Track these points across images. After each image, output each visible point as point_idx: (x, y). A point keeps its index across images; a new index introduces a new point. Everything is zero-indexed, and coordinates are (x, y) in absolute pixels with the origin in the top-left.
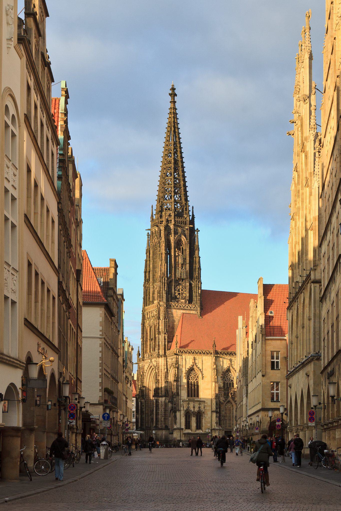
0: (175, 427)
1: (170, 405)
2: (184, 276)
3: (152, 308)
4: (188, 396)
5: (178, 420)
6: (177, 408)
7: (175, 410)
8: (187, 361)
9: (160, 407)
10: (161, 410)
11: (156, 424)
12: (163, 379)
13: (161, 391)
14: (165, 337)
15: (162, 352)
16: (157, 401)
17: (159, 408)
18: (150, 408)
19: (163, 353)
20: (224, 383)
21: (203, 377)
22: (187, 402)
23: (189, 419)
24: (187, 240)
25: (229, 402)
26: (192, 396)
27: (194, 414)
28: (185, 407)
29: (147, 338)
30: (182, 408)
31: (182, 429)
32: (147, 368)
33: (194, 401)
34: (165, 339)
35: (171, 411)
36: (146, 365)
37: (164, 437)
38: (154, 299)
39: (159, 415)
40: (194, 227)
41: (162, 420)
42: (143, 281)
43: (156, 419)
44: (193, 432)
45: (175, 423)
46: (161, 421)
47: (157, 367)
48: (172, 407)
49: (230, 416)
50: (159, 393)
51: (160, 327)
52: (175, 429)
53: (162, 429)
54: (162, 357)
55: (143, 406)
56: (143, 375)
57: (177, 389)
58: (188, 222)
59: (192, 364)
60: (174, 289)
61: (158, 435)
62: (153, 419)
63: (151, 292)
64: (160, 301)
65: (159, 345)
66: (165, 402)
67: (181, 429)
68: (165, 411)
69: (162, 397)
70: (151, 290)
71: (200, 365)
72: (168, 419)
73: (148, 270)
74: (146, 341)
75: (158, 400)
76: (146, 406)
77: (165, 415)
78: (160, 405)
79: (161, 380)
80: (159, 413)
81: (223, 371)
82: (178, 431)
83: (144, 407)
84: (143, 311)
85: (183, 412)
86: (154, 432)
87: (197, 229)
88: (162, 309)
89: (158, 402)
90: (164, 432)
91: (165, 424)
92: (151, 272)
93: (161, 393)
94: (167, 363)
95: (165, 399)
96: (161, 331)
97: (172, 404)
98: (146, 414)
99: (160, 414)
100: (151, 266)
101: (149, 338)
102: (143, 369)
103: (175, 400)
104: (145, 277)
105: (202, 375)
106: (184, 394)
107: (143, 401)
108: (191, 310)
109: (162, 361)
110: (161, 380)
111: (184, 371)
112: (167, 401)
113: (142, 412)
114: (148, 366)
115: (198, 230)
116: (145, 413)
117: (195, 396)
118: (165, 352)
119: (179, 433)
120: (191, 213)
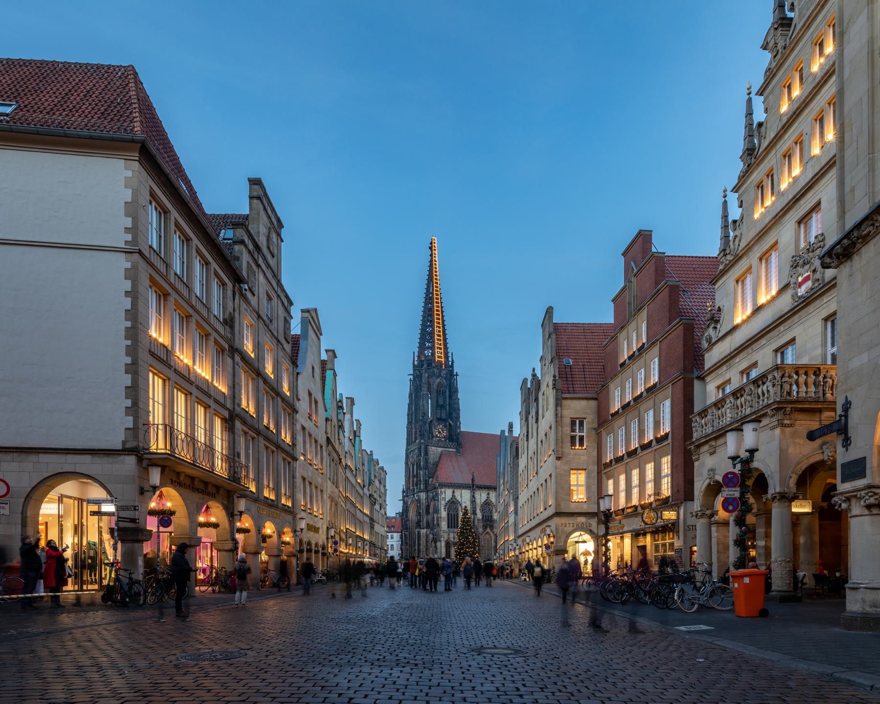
2: (444, 416)
3: (413, 447)
5: (439, 550)
7: (435, 540)
8: (448, 494)
16: (419, 533)
38: (416, 439)
40: (452, 371)
43: (419, 549)
47: (419, 501)
57: (438, 521)
71: (459, 498)
84: (407, 449)
85: (443, 544)
88: (423, 446)
106: (444, 525)
109: (423, 495)
115: (457, 375)
118: (426, 488)
120: (450, 359)
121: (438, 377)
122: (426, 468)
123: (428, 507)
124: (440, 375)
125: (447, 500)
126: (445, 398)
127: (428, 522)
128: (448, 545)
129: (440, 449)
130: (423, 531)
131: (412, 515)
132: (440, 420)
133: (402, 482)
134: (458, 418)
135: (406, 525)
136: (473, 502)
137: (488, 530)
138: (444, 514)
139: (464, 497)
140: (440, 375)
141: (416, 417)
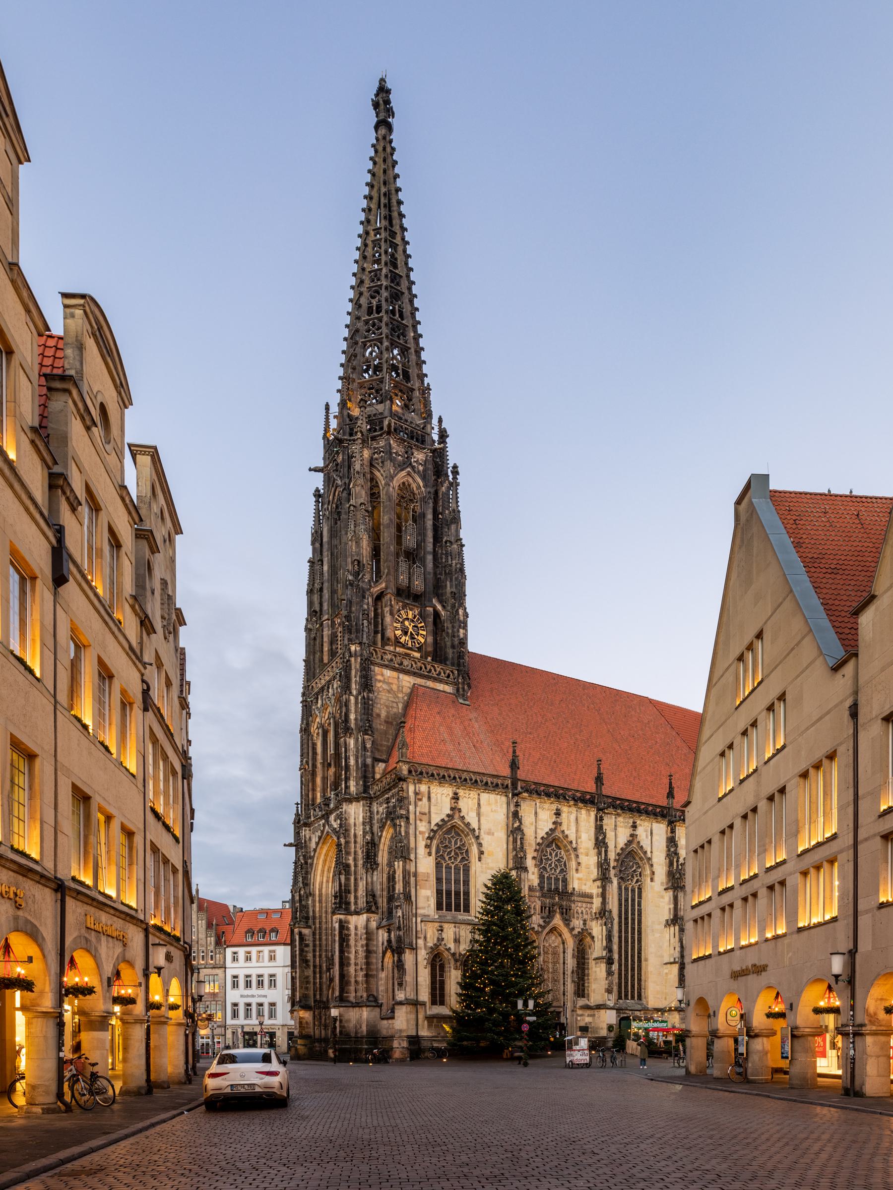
0: (400, 996)
1: (382, 936)
4: (439, 907)
5: (409, 978)
6: (407, 941)
7: (398, 948)
9: (352, 942)
10: (356, 952)
11: (342, 990)
12: (360, 862)
13: (356, 897)
14: (364, 742)
16: (343, 926)
17: (348, 946)
18: (326, 951)
19: (361, 789)
20: (541, 877)
21: (482, 853)
22: (437, 925)
23: (442, 976)
24: (425, 486)
25: (554, 929)
26: (449, 908)
27: (456, 961)
28: (428, 939)
30: (421, 942)
31: (423, 1004)
32: (317, 844)
33: (455, 922)
35: (384, 953)
36: (313, 836)
37: (364, 1028)
39: (349, 964)
41: (360, 979)
42: (305, 615)
43: (342, 976)
46: (356, 982)
47: (344, 829)
48: (389, 941)
49: (555, 971)
50: (348, 904)
51: (352, 716)
52: (401, 1003)
53: (357, 1005)
54: (357, 799)
55: (307, 946)
56: (306, 863)
57: (406, 883)
59: (449, 812)
60: (392, 614)
61: (348, 1021)
62: (331, 980)
63: (326, 639)
64: (350, 640)
65: (347, 767)
66: (367, 927)
67: (415, 1004)
68: (369, 952)
69: (357, 913)
71: (471, 818)
72: (377, 976)
73: (317, 586)
75: (348, 922)
76: (314, 946)
77: (368, 964)
79: (356, 866)
80: (349, 958)
81: (539, 840)
82: (409, 1008)
83: (311, 948)
85: (423, 954)
87: (455, 467)
89: (348, 929)
90: (365, 1014)
91: (367, 989)
92: (326, 585)
93: (356, 903)
94: (371, 818)
95: (368, 920)
96: (353, 726)
97: (389, 932)
98: (315, 966)
99: (352, 961)
102: (306, 846)
103: (400, 913)
104: (310, 604)
105: (480, 845)
106: (426, 898)
107: (306, 931)
109: (355, 812)
110: (356, 866)
112: (373, 925)
113: (304, 961)
114: (320, 838)
116: (311, 964)
117: (458, 909)
118: (366, 788)
119: (413, 1016)
121: (401, 467)
122: (367, 727)
123: (371, 848)
124: (407, 463)
125: (436, 819)
126: (422, 533)
127: (371, 895)
128: (437, 962)
130: (357, 922)
131: (323, 880)
132: (405, 594)
134: (459, 596)
135: (304, 908)
136: (515, 832)
137: (557, 920)
138: (425, 864)
139: (488, 812)
140: (407, 463)
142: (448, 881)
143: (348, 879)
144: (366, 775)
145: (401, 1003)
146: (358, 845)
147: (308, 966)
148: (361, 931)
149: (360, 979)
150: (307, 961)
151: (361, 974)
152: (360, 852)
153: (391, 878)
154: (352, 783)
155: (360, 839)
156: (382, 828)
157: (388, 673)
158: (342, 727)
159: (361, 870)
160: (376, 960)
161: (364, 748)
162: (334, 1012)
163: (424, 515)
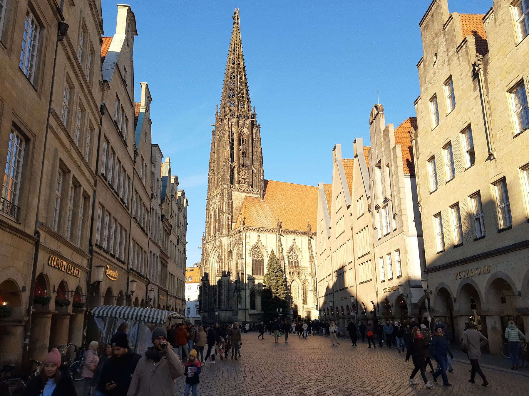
0: (240, 307)
2: (246, 163)
8: (251, 238)
9: (223, 287)
12: (226, 258)
14: (228, 217)
15: (225, 232)
17: (222, 288)
27: (259, 293)
29: (211, 222)
34: (228, 219)
41: (226, 300)
44: (258, 312)
45: (240, 303)
48: (236, 286)
51: (224, 208)
52: (240, 310)
54: (226, 236)
58: (250, 117)
62: (215, 300)
65: (222, 225)
67: (245, 310)
68: (229, 290)
70: (216, 177)
71: (264, 243)
74: (210, 224)
77: (229, 295)
78: (223, 285)
86: (216, 313)
88: (226, 191)
89: (222, 282)
91: (228, 304)
100: (216, 156)
101: (212, 220)
108: (254, 194)
109: (225, 241)
111: (248, 248)
118: (229, 232)
123: (231, 252)
129: (243, 195)
133: (202, 229)
139: (270, 242)
141: (218, 164)
142: (256, 265)
143: (222, 264)
144: (230, 228)
145: (240, 310)
146: (226, 252)
147: (206, 295)
148: (226, 283)
149: (226, 300)
150: (206, 293)
151: (226, 299)
152: (226, 254)
153: (237, 264)
154: (224, 231)
155: (226, 250)
156: (234, 246)
157: (236, 193)
158: (221, 211)
159: (227, 261)
160: (231, 293)
161: (228, 219)
162: (216, 313)
163: (248, 140)
